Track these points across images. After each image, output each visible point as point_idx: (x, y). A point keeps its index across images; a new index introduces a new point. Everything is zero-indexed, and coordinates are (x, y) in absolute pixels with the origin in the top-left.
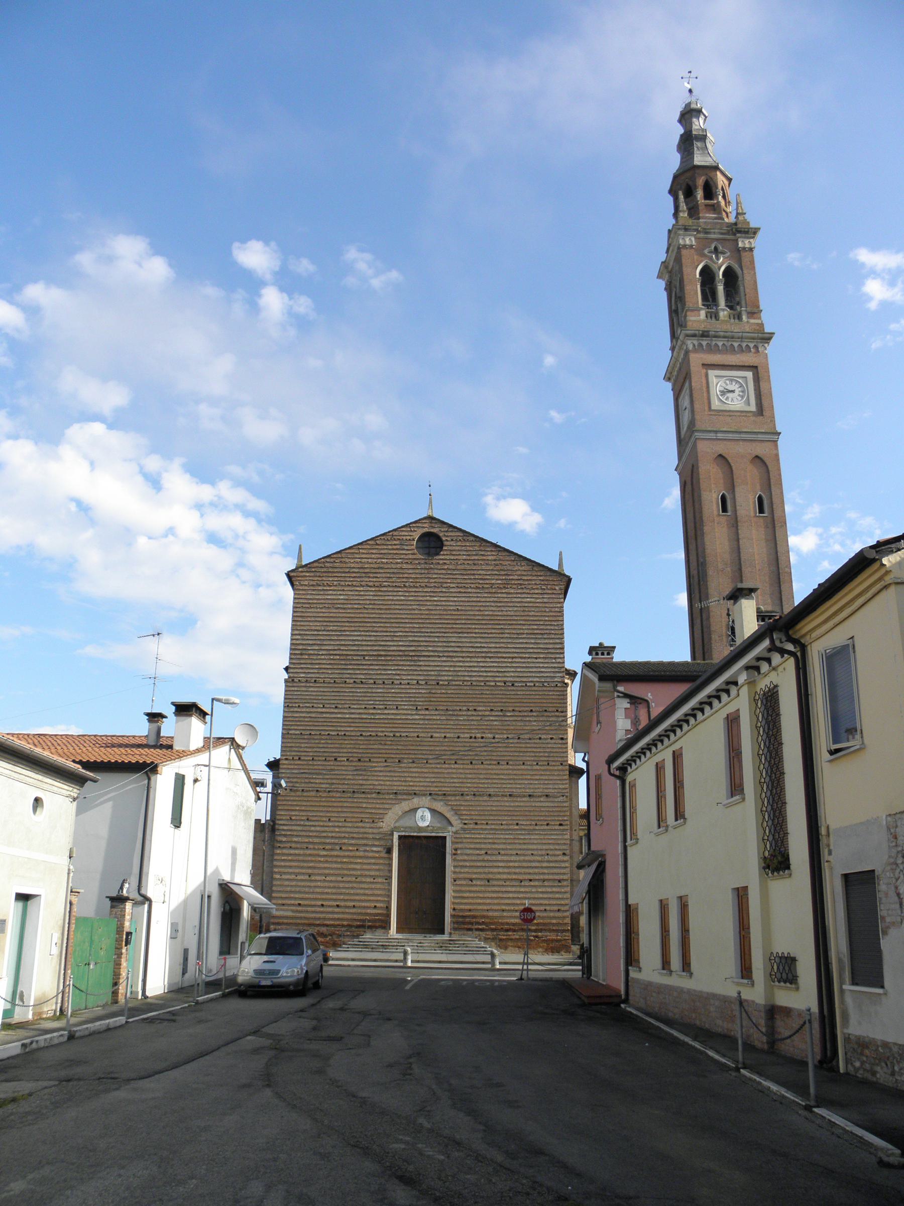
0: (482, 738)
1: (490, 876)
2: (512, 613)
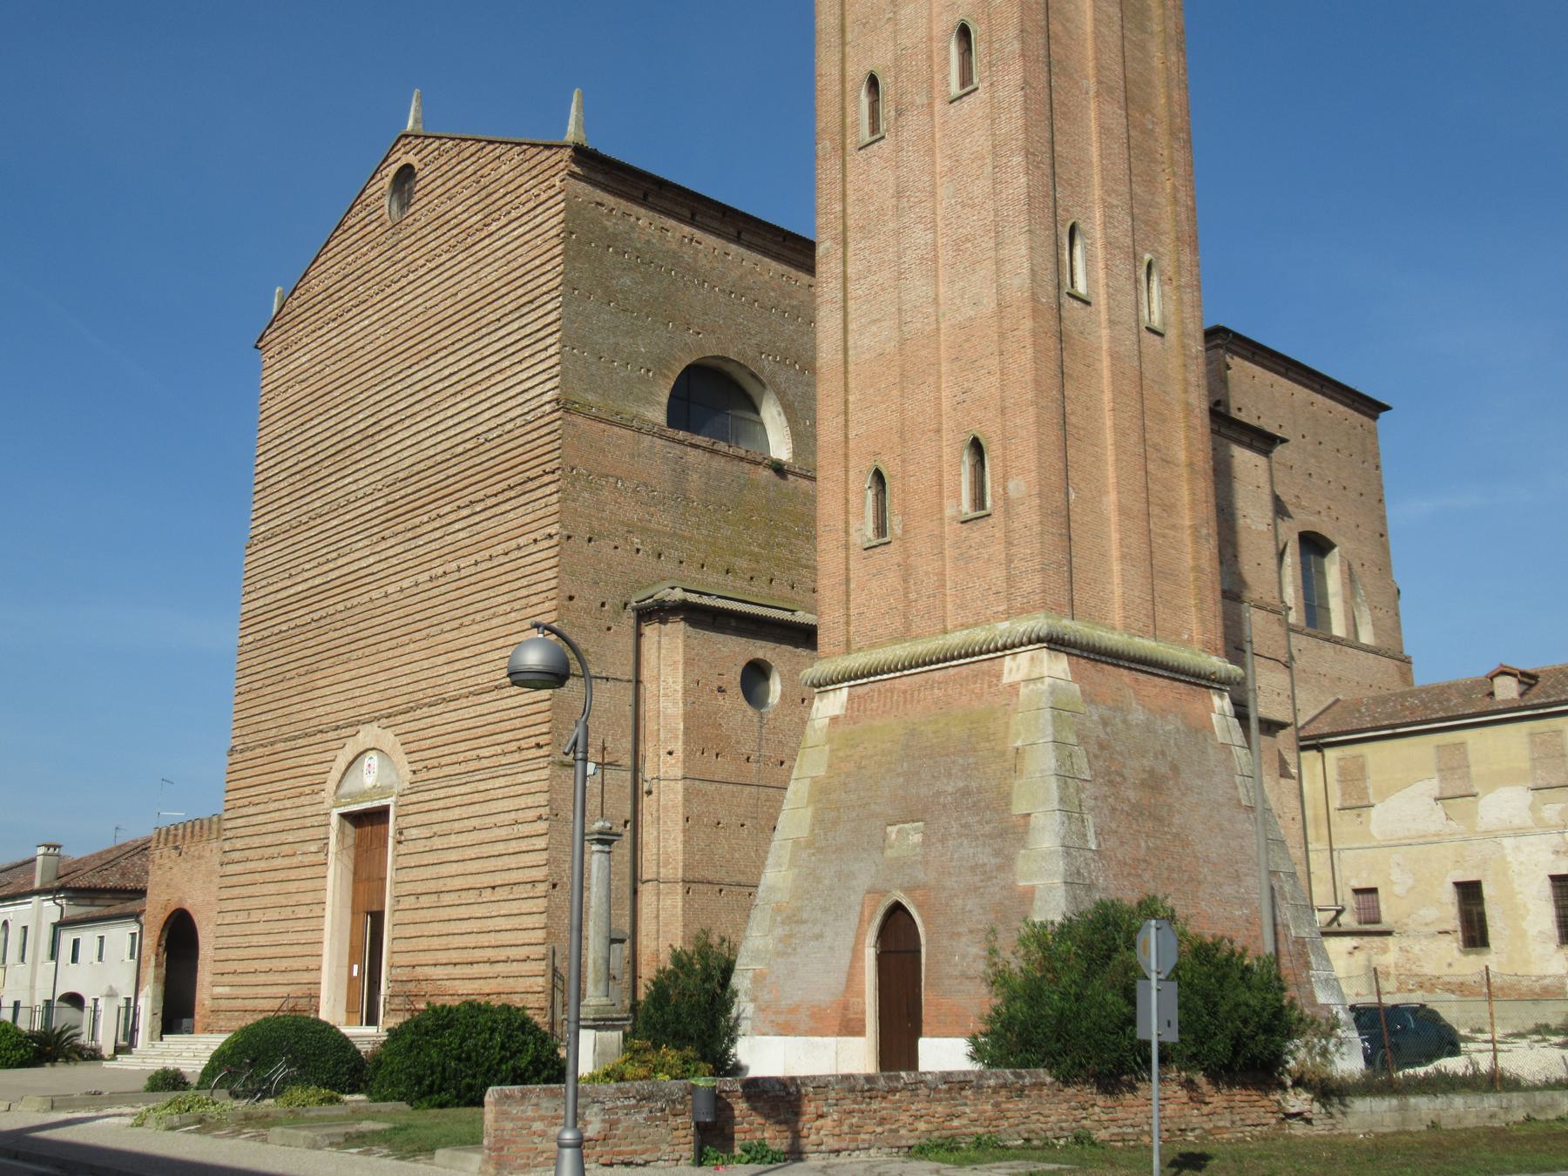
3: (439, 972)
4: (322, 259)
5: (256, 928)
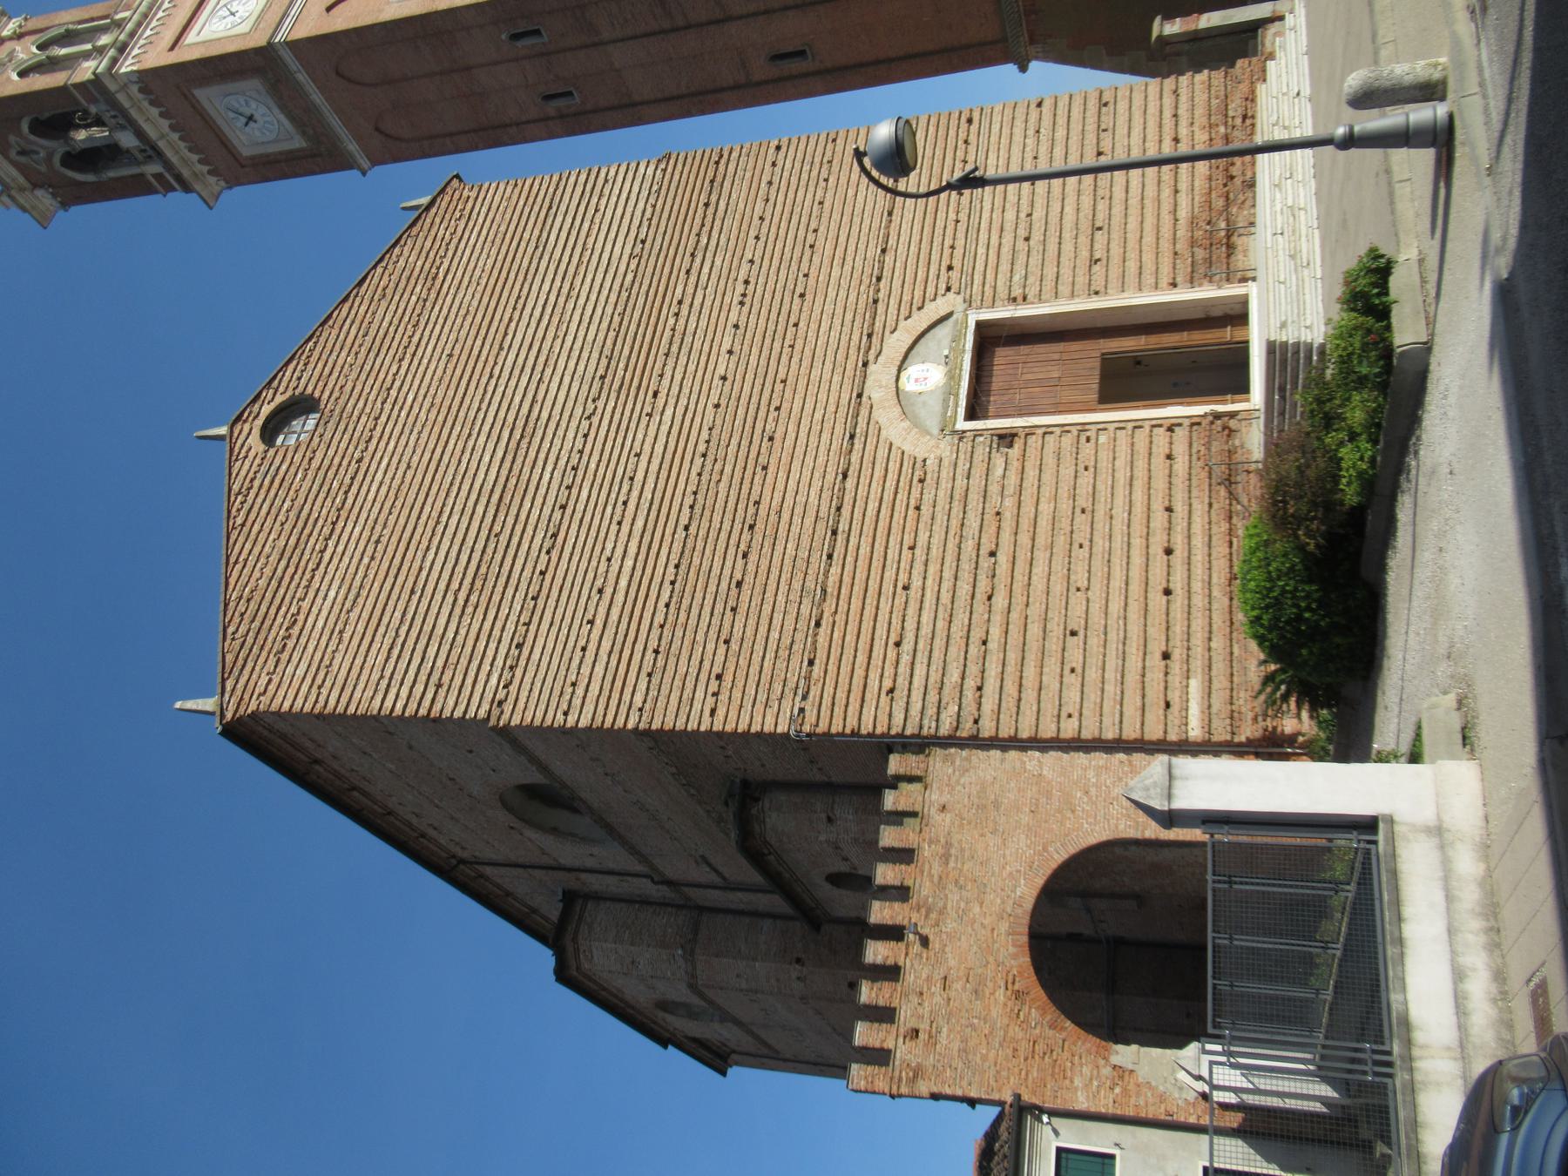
0: (747, 282)
1: (1085, 226)
2: (490, 262)
3: (1183, 213)
4: (232, 581)
5: (1096, 608)
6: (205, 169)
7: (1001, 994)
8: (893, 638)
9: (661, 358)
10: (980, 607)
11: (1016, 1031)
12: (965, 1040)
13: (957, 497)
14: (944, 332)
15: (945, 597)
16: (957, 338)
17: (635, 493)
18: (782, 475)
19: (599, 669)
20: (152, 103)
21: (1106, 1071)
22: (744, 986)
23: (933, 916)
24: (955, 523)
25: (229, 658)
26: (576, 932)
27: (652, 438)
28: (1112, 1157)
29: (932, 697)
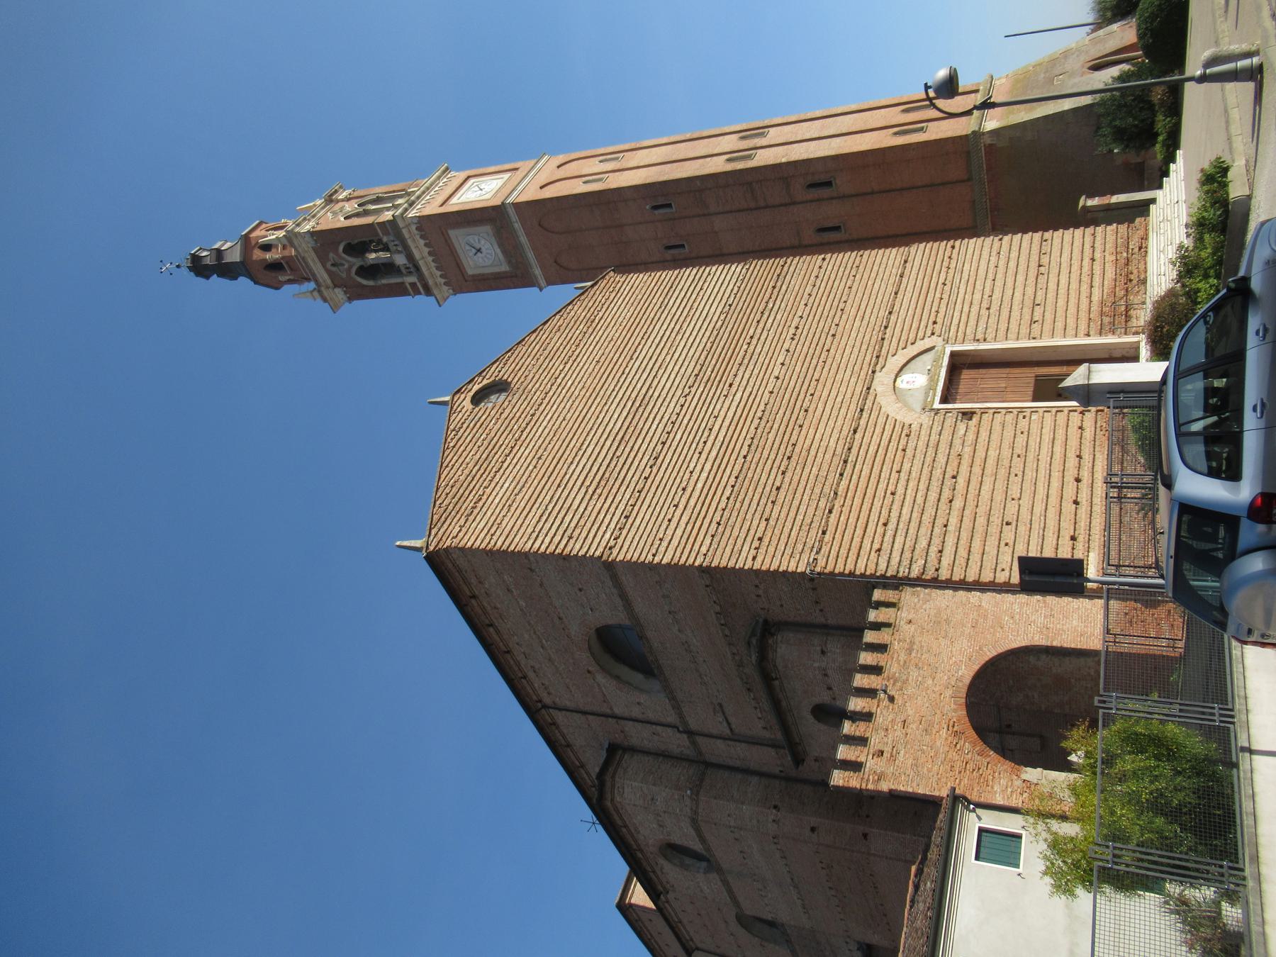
4: (443, 476)
6: (443, 281)
7: (944, 733)
8: (882, 520)
9: (736, 366)
10: (943, 506)
11: (953, 755)
12: (916, 759)
13: (931, 445)
14: (928, 358)
15: (920, 500)
16: (937, 361)
17: (712, 437)
18: (812, 431)
19: (679, 532)
20: (422, 237)
21: (1018, 783)
22: (732, 823)
23: (899, 684)
24: (929, 459)
25: (436, 517)
26: (614, 774)
27: (727, 409)
28: (1019, 837)
29: (907, 555)
